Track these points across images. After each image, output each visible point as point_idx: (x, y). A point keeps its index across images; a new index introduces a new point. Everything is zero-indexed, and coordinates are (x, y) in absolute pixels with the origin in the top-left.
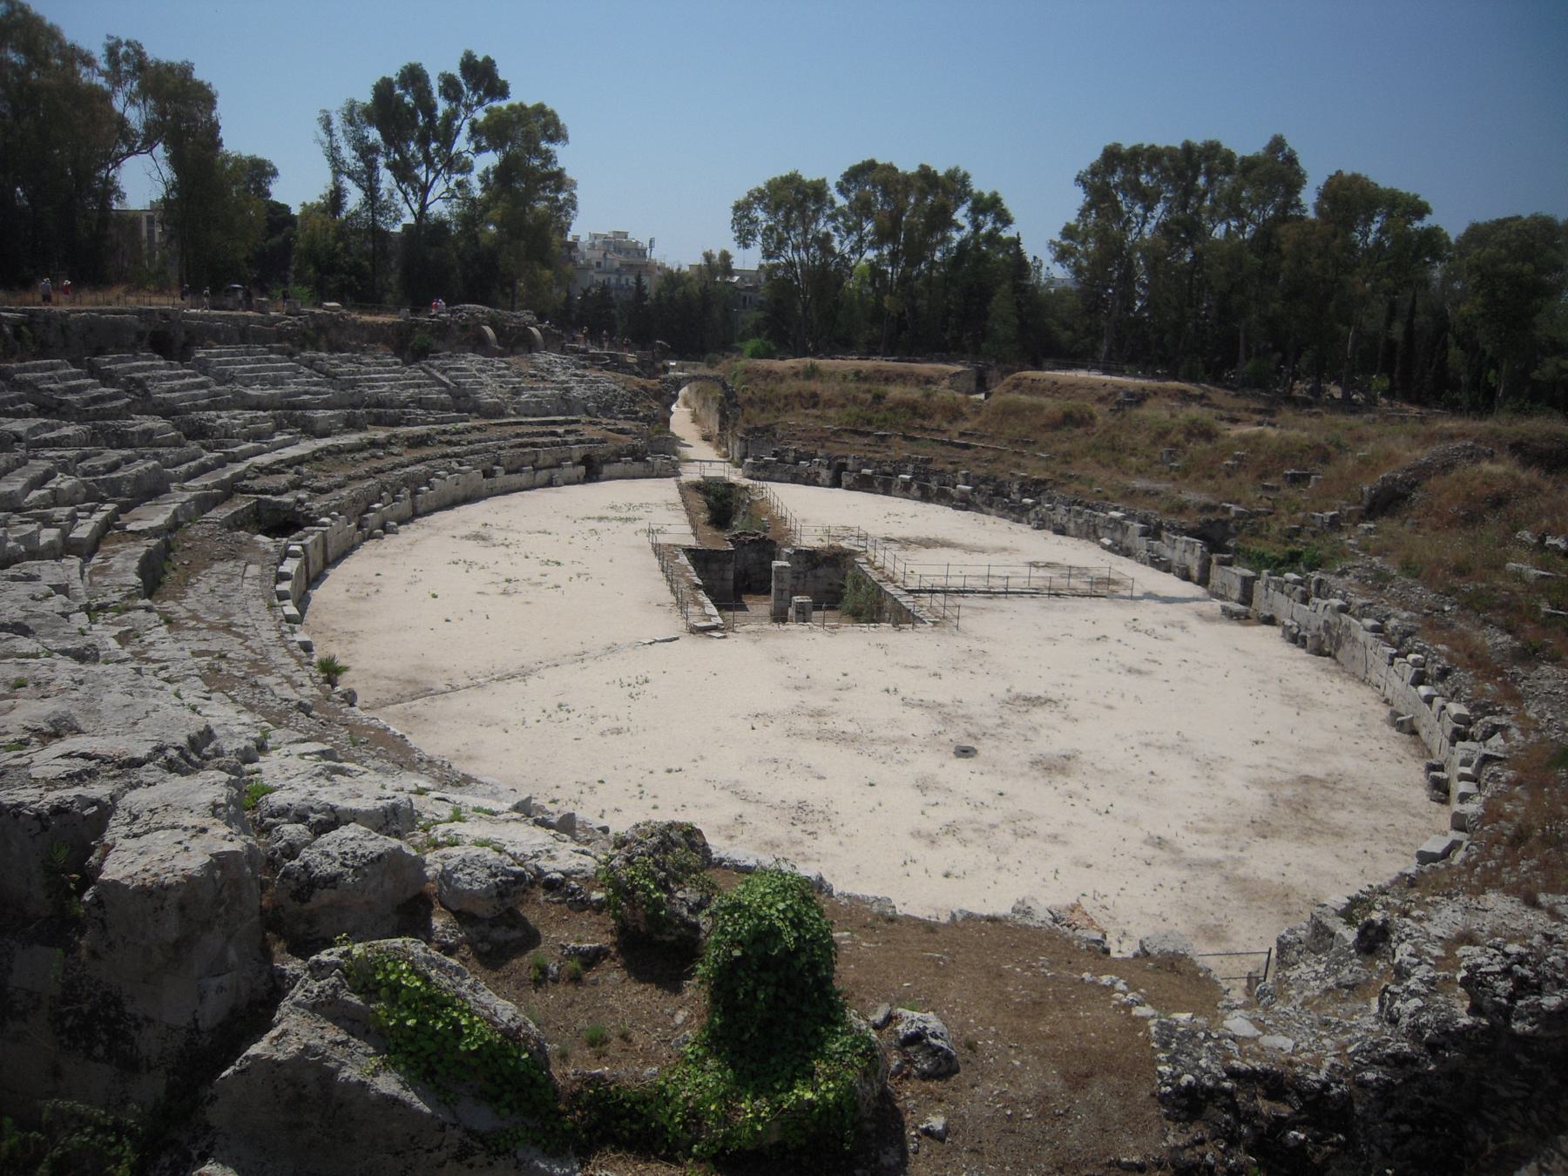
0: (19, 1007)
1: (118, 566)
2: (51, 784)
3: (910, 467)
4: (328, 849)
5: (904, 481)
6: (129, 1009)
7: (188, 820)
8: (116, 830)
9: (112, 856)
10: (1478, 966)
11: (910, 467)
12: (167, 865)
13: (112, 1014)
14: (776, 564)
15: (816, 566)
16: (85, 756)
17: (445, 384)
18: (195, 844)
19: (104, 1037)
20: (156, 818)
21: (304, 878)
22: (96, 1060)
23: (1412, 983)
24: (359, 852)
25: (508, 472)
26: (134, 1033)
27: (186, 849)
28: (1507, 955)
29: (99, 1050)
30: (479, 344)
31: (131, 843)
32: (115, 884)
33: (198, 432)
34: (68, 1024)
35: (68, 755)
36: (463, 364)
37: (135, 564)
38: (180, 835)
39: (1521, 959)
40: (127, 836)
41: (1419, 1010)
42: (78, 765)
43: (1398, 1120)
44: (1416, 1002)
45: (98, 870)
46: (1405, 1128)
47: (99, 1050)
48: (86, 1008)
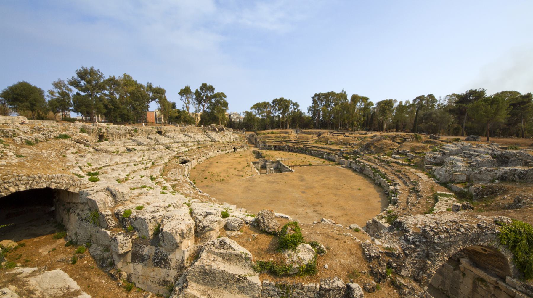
2: (151, 213)
8: (165, 222)
10: (425, 230)
16: (157, 206)
18: (182, 222)
23: (410, 233)
28: (431, 227)
29: (163, 266)
31: (169, 223)
32: (166, 232)
38: (178, 221)
39: (434, 228)
41: (413, 239)
42: (156, 208)
43: (413, 260)
44: (412, 237)
45: (162, 229)
46: (415, 262)
47: (163, 266)
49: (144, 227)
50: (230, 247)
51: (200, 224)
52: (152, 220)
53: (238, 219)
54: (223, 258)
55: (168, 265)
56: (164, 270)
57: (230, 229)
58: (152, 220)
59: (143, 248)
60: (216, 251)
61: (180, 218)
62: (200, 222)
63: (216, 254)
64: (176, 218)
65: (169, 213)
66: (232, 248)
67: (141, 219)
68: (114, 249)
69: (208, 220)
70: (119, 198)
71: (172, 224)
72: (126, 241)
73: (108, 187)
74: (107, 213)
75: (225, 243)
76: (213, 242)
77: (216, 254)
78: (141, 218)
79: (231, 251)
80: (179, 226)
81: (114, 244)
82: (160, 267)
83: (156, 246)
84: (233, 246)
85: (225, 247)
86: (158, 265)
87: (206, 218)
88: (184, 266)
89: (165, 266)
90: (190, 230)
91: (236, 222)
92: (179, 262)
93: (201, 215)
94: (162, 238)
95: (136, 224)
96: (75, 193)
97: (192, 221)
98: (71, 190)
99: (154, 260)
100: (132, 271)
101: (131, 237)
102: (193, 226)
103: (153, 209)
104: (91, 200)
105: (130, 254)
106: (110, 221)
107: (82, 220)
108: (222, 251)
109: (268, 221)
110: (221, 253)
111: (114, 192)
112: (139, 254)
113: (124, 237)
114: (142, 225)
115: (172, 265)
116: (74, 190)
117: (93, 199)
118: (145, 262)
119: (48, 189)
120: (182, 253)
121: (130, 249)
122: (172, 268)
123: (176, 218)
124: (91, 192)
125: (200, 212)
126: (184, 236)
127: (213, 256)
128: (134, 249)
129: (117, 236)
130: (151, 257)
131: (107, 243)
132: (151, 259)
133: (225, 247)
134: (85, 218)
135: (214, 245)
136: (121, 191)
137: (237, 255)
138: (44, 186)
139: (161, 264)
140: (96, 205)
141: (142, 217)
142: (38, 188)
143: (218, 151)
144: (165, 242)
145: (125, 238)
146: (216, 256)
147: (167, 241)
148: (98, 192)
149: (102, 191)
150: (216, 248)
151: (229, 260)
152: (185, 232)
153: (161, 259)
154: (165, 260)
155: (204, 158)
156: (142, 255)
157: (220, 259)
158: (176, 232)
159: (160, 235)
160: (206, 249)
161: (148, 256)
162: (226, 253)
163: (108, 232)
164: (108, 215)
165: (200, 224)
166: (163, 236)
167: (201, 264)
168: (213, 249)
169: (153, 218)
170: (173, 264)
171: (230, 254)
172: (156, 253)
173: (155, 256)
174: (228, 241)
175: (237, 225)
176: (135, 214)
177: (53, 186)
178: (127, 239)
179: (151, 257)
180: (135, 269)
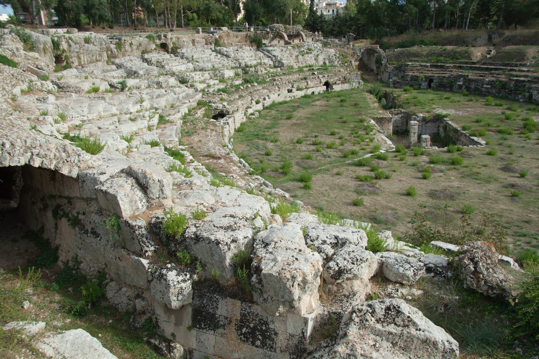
0: (222, 323)
1: (169, 133)
3: (462, 79)
4: (344, 256)
5: (460, 85)
6: (271, 326)
9: (263, 262)
11: (462, 79)
12: (292, 267)
13: (264, 328)
14: (412, 122)
15: (426, 123)
16: (232, 216)
17: (269, 57)
19: (260, 338)
20: (277, 245)
21: (337, 269)
22: (257, 347)
24: (358, 258)
25: (297, 90)
26: (273, 336)
27: (297, 259)
29: (258, 343)
32: (271, 275)
33: (183, 81)
34: (244, 330)
36: (276, 48)
40: (267, 253)
47: (258, 343)
48: (252, 325)
49: (216, 258)
50: (409, 322)
52: (233, 246)
54: (394, 344)
55: (269, 342)
56: (261, 350)
57: (392, 278)
58: (233, 246)
59: (217, 301)
60: (379, 326)
61: (293, 247)
63: (378, 334)
66: (415, 324)
67: (210, 241)
68: (158, 296)
69: (347, 257)
71: (279, 258)
72: (183, 285)
73: (130, 168)
75: (399, 312)
76: (370, 306)
77: (378, 334)
78: (208, 239)
79: (413, 331)
81: (159, 287)
82: (253, 344)
83: (243, 300)
84: (416, 320)
85: (399, 320)
86: (248, 339)
88: (305, 350)
89: (263, 345)
92: (295, 341)
94: (257, 285)
95: (198, 250)
96: (72, 178)
98: (65, 171)
99: (240, 328)
100: (194, 344)
101: (191, 277)
104: (106, 193)
105: (190, 310)
106: (144, 239)
107: (86, 232)
108: (392, 328)
109: (487, 269)
110: (390, 333)
111: (143, 181)
112: (209, 313)
113: (178, 275)
114: (212, 255)
115: (279, 344)
116: (70, 172)
118: (221, 330)
119: (27, 167)
120: (300, 324)
121: (190, 301)
122: (278, 350)
124: (103, 178)
127: (372, 336)
128: (197, 302)
129: (164, 271)
130: (234, 322)
131: (142, 283)
132: (233, 327)
133: (399, 320)
134: (92, 229)
135: (373, 313)
137: (426, 342)
138: (23, 161)
139: (255, 338)
140: (118, 205)
141: (213, 238)
142: (12, 165)
144: (265, 296)
145: (180, 278)
146: (378, 338)
147: (271, 293)
150: (378, 321)
151: (405, 349)
153: (255, 328)
154: (263, 333)
156: (214, 315)
157: (386, 344)
160: (357, 320)
161: (226, 318)
162: (401, 335)
163: (145, 262)
164: (140, 227)
166: (260, 281)
167: (348, 351)
168: (372, 321)
169: (234, 241)
170: (281, 341)
171: (411, 338)
172: (243, 315)
173: (241, 321)
174: (406, 308)
176: (194, 229)
177: (37, 164)
178: (184, 281)
179: (234, 322)
180: (199, 341)
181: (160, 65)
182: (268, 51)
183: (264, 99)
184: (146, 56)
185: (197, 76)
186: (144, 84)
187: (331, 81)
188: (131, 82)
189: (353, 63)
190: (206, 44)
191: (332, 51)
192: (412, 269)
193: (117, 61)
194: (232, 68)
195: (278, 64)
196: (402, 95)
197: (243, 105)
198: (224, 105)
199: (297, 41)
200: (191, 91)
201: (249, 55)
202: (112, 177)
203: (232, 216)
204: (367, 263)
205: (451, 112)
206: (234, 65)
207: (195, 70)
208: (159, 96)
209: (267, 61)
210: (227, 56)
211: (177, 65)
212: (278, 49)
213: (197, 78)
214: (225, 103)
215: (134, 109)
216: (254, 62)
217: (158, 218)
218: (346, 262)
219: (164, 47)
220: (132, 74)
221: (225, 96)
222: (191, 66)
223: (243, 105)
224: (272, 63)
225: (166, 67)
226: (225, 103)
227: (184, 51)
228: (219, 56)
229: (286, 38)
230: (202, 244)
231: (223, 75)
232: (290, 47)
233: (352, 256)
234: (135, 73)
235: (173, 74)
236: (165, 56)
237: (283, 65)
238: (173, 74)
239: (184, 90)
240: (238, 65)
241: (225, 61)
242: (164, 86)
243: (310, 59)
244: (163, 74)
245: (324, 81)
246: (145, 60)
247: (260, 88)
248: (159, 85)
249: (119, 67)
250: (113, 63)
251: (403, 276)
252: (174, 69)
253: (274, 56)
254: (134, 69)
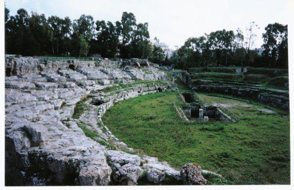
2: (68, 155)
7: (97, 163)
8: (82, 165)
14: (200, 110)
16: (73, 150)
30: (136, 65)
31: (85, 168)
32: (83, 176)
33: (80, 85)
35: (70, 150)
37: (69, 112)
38: (95, 166)
45: (79, 174)
51: (117, 172)
53: (158, 171)
62: (117, 170)
64: (93, 162)
65: (85, 158)
70: (35, 139)
71: (89, 169)
74: (23, 153)
80: (96, 171)
87: (124, 166)
90: (106, 177)
91: (156, 174)
93: (118, 162)
97: (108, 167)
102: (110, 173)
103: (69, 152)
117: (11, 137)
123: (93, 162)
125: (117, 159)
126: (100, 182)
136: (38, 131)
141: (59, 160)
143: (139, 92)
148: (15, 130)
149: (18, 130)
152: (102, 178)
155: (122, 99)
158: (93, 177)
159: (75, 179)
164: (24, 156)
165: (117, 172)
175: (157, 177)
181: (68, 76)
182: (129, 72)
183: (125, 96)
184: (60, 71)
185: (88, 82)
186: (56, 85)
187: (161, 88)
188: (47, 85)
189: (174, 79)
190: (96, 66)
191: (163, 73)
192: (158, 176)
193: (43, 73)
194: (109, 79)
195: (134, 78)
196: (201, 97)
197: (112, 98)
198: (101, 99)
199: (145, 67)
200: (84, 90)
201: (118, 74)
202: (15, 130)
203: (73, 150)
204: (135, 172)
205: (225, 106)
206: (110, 78)
207: (88, 79)
208: (64, 92)
209: (128, 76)
210: (107, 73)
211: (77, 76)
212: (135, 71)
213: (88, 84)
214: (102, 97)
215: (47, 98)
216: (121, 77)
217: (35, 151)
218: (124, 172)
219: (72, 67)
220: (50, 80)
221: (103, 93)
222: (85, 77)
223: (112, 98)
224: (131, 78)
225: (71, 77)
226: (102, 97)
227: (82, 69)
228: (102, 73)
229: (139, 65)
230: (53, 163)
231: (103, 82)
232: (141, 70)
233: (128, 168)
234: (52, 79)
235: (74, 81)
236: (70, 72)
237: (136, 79)
238: (74, 81)
239: (80, 89)
240: (112, 78)
241: (105, 76)
242: (68, 86)
243: (150, 77)
244: (69, 81)
245: (157, 87)
246: (58, 73)
247: (123, 90)
248: (65, 87)
249: (43, 76)
250: (40, 74)
251: (154, 179)
252: (76, 78)
253: (132, 74)
254: (52, 77)
